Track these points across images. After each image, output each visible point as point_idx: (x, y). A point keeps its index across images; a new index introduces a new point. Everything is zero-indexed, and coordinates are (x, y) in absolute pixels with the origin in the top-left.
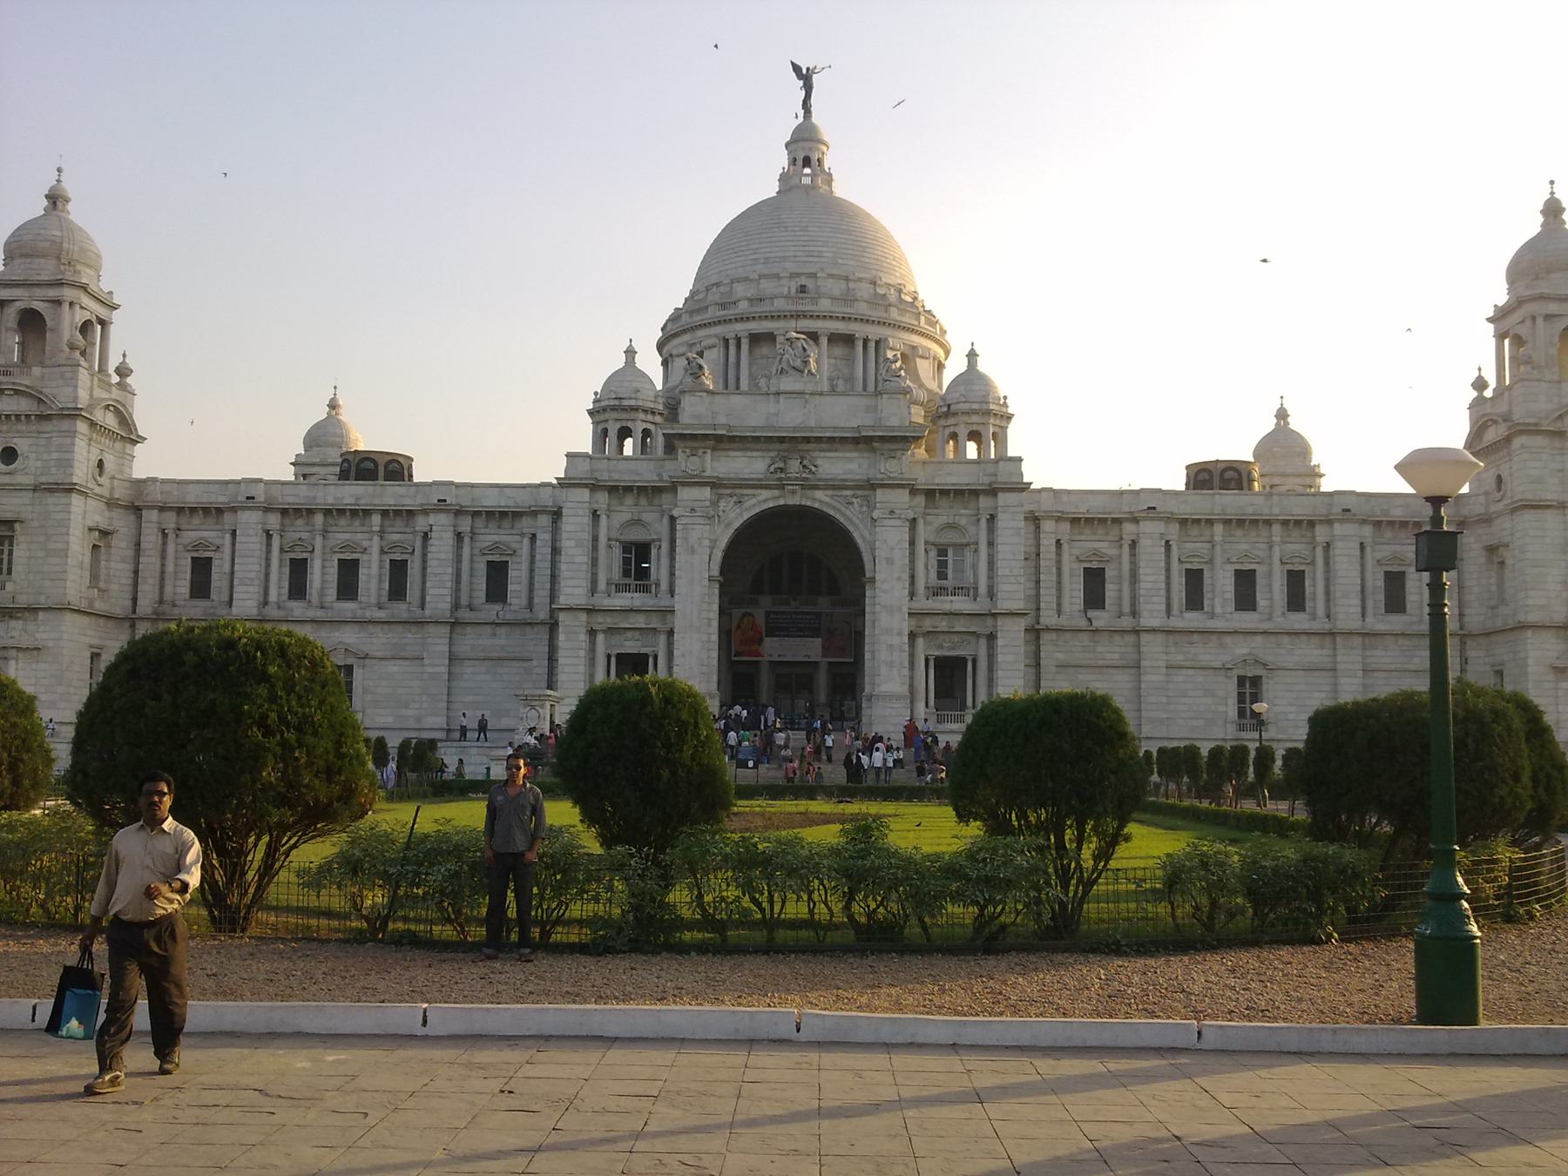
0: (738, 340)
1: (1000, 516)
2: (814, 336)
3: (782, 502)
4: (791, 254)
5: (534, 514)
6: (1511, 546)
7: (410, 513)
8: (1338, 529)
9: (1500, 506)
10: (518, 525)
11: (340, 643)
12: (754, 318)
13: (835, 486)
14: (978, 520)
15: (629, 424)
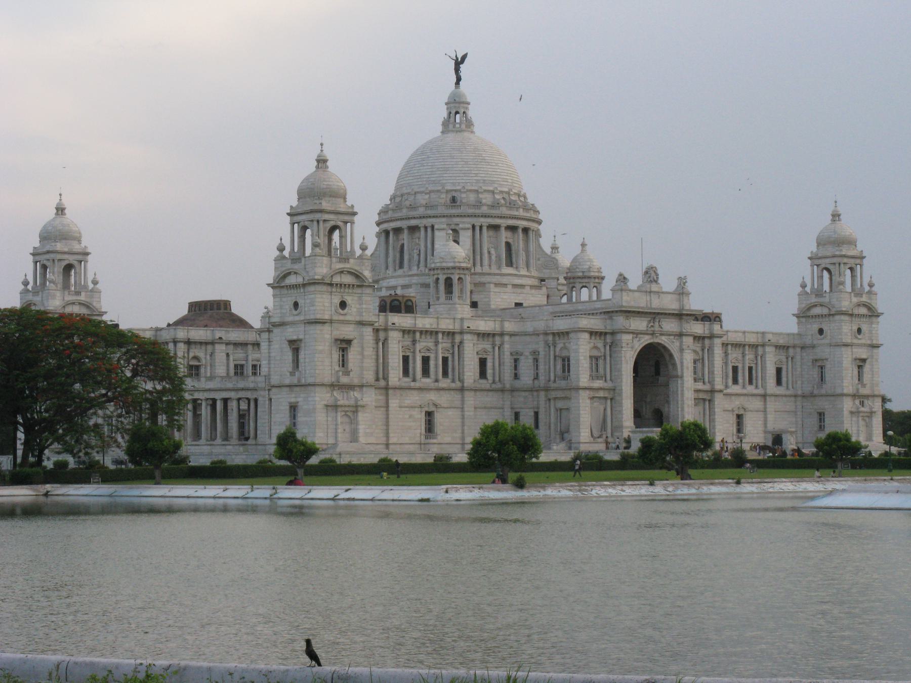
0: (481, 227)
1: (715, 348)
2: (512, 229)
3: (652, 341)
4: (495, 179)
5: (502, 334)
6: (829, 360)
7: (454, 333)
8: (768, 349)
9: (826, 341)
10: (491, 339)
11: (432, 400)
12: (492, 216)
13: (669, 334)
14: (703, 350)
15: (462, 276)
